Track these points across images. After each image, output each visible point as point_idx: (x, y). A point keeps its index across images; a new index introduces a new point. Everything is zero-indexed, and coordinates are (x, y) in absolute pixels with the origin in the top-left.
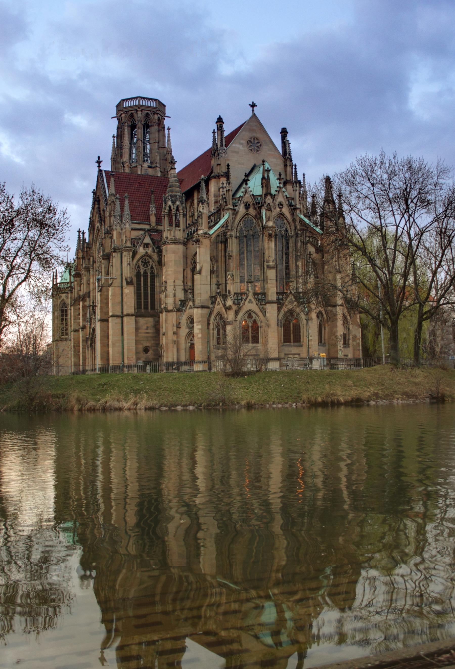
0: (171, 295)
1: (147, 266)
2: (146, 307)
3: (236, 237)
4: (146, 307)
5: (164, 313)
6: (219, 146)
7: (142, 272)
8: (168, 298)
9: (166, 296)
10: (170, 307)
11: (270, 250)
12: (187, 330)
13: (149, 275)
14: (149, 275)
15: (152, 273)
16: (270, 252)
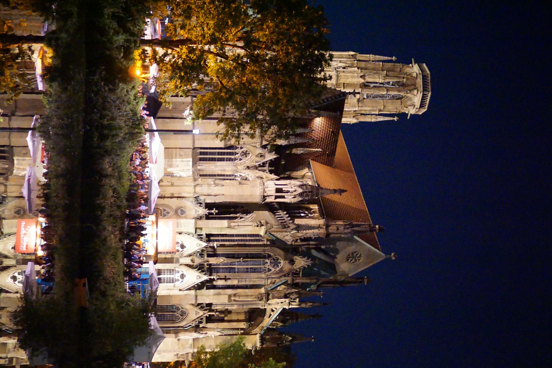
0: (210, 192)
1: (243, 155)
2: (201, 153)
3: (264, 251)
4: (201, 153)
5: (193, 184)
6: (355, 229)
7: (237, 151)
8: (207, 188)
9: (209, 185)
10: (198, 189)
11: (246, 297)
12: (174, 207)
13: (233, 157)
14: (233, 157)
15: (235, 159)
16: (243, 297)
